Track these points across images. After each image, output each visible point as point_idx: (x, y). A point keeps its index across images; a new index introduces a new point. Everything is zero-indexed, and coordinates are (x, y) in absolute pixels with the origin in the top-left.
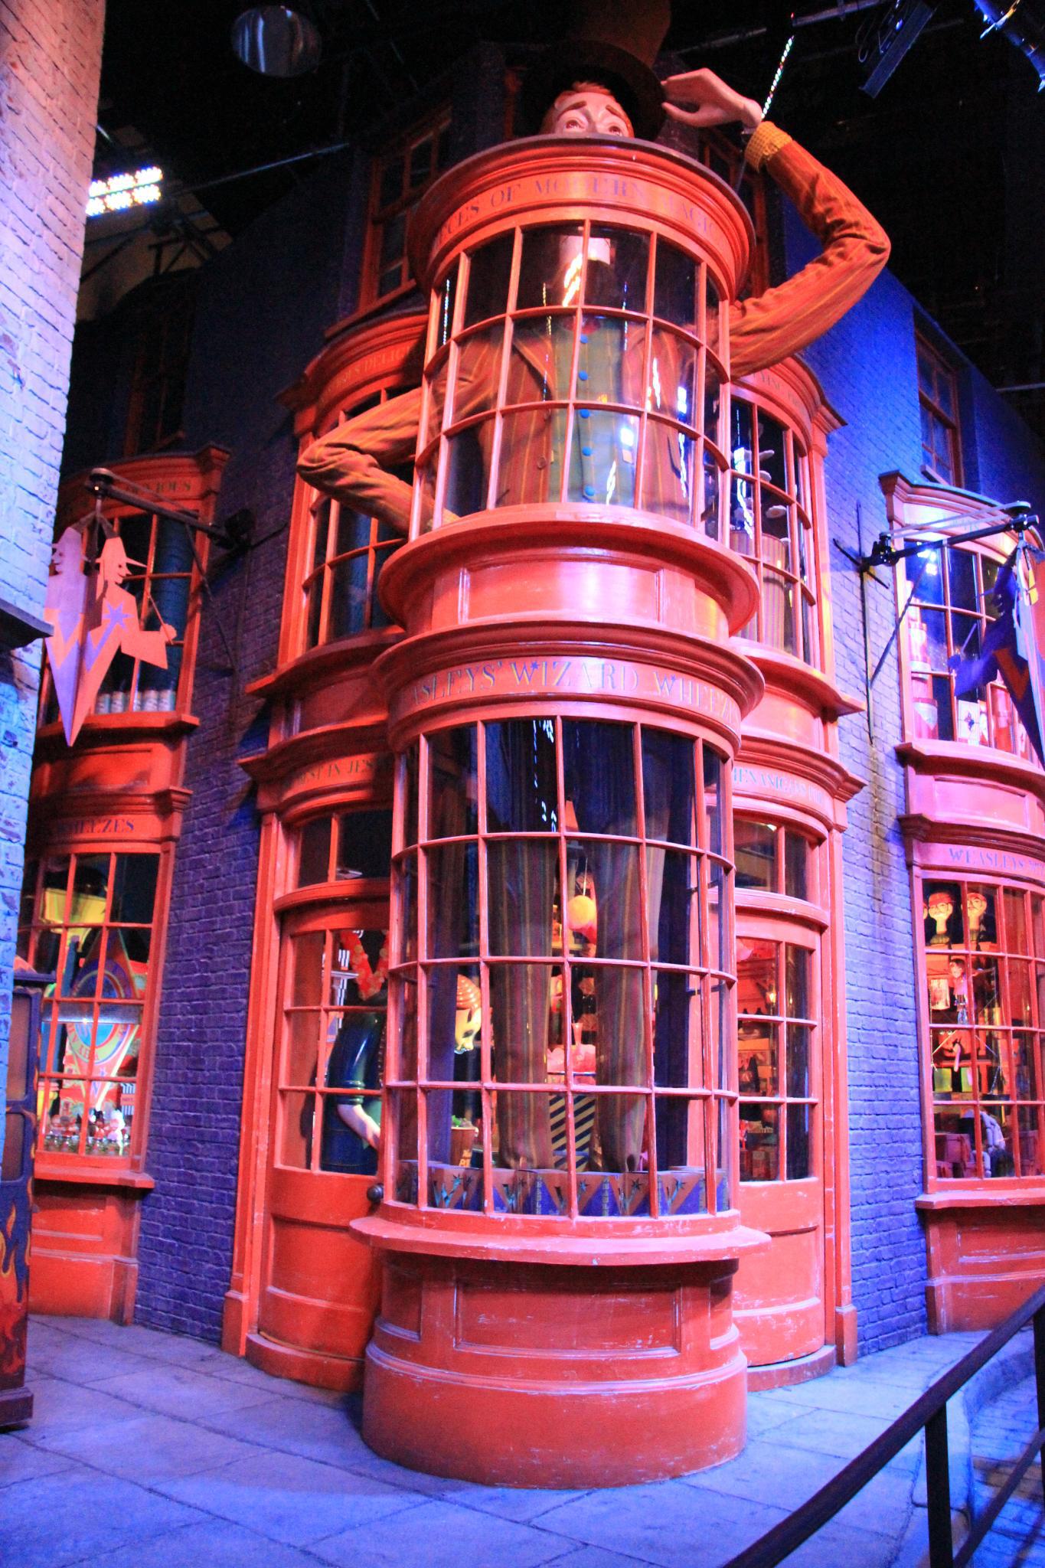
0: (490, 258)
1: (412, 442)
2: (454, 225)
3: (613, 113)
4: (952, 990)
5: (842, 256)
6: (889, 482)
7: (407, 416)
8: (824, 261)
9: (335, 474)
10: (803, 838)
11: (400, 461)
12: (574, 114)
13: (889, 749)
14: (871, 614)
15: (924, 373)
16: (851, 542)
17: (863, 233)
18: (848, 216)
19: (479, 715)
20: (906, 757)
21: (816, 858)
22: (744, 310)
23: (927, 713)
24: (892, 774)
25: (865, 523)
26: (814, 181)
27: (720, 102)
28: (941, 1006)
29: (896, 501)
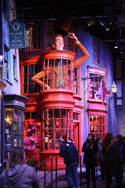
0: (52, 61)
1: (43, 78)
2: (47, 56)
3: (62, 40)
4: (94, 128)
5: (85, 57)
6: (88, 67)
7: (42, 75)
8: (83, 57)
9: (36, 81)
10: (77, 114)
11: (41, 79)
12: (58, 41)
13: (86, 101)
14: (85, 85)
15: (94, 45)
16: (83, 77)
17: (87, 55)
18: (85, 53)
19: (53, 108)
20: (88, 101)
21: (79, 115)
22: (75, 63)
23: (91, 95)
24: (87, 104)
25: (85, 73)
26: (82, 48)
27: (73, 36)
28: (92, 130)
29: (89, 69)
